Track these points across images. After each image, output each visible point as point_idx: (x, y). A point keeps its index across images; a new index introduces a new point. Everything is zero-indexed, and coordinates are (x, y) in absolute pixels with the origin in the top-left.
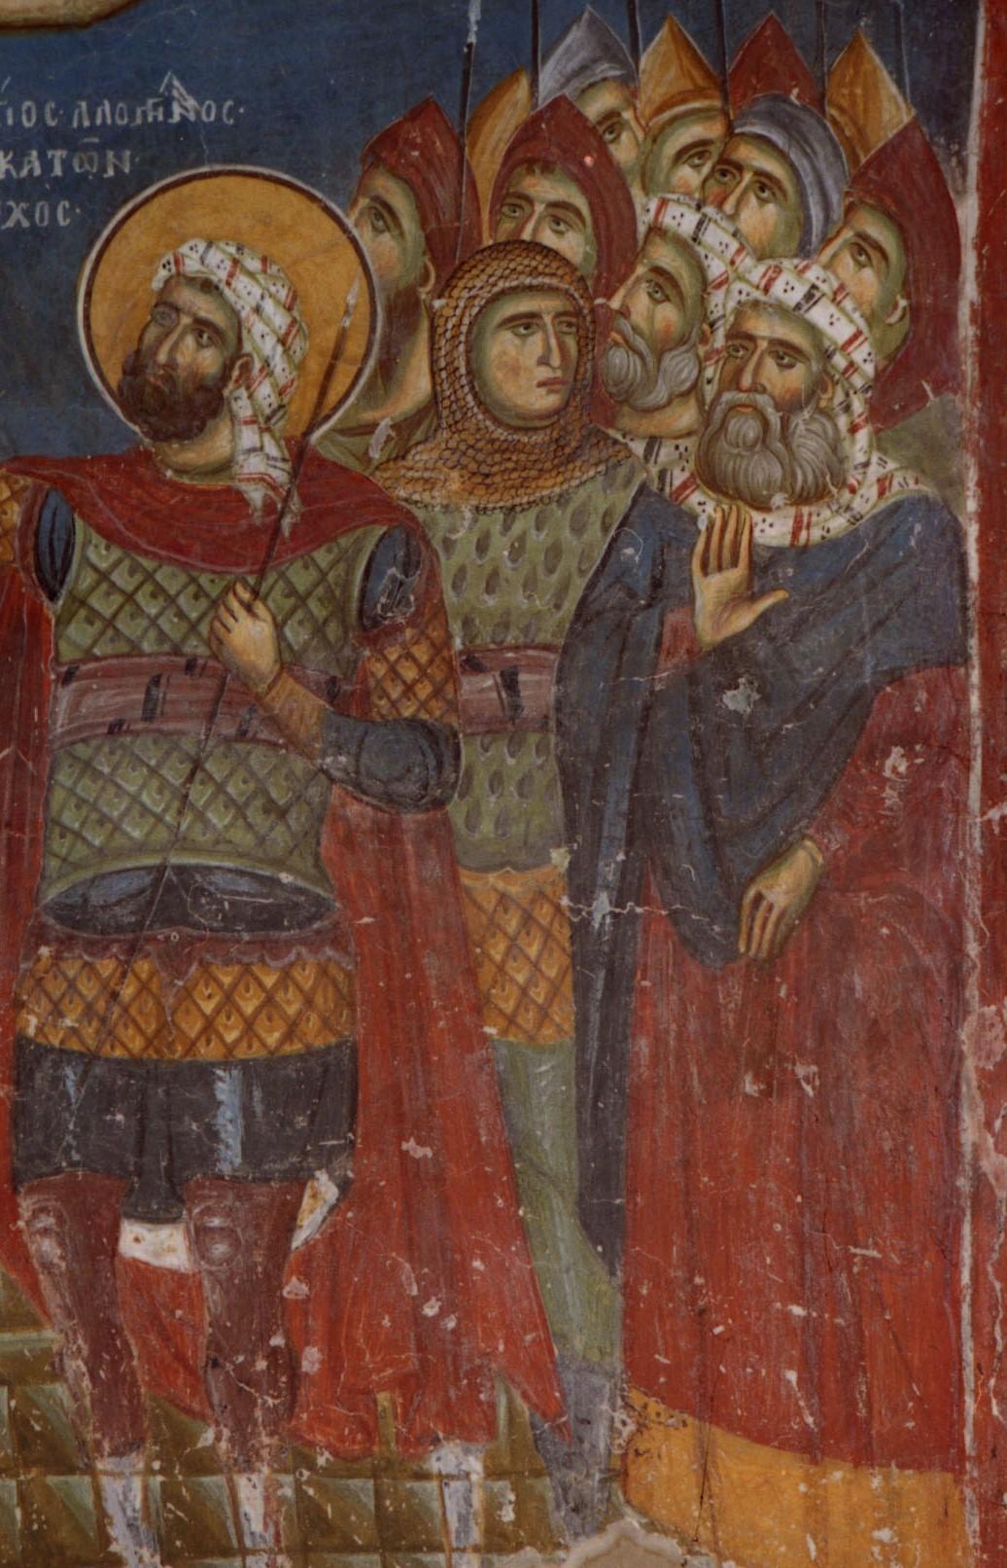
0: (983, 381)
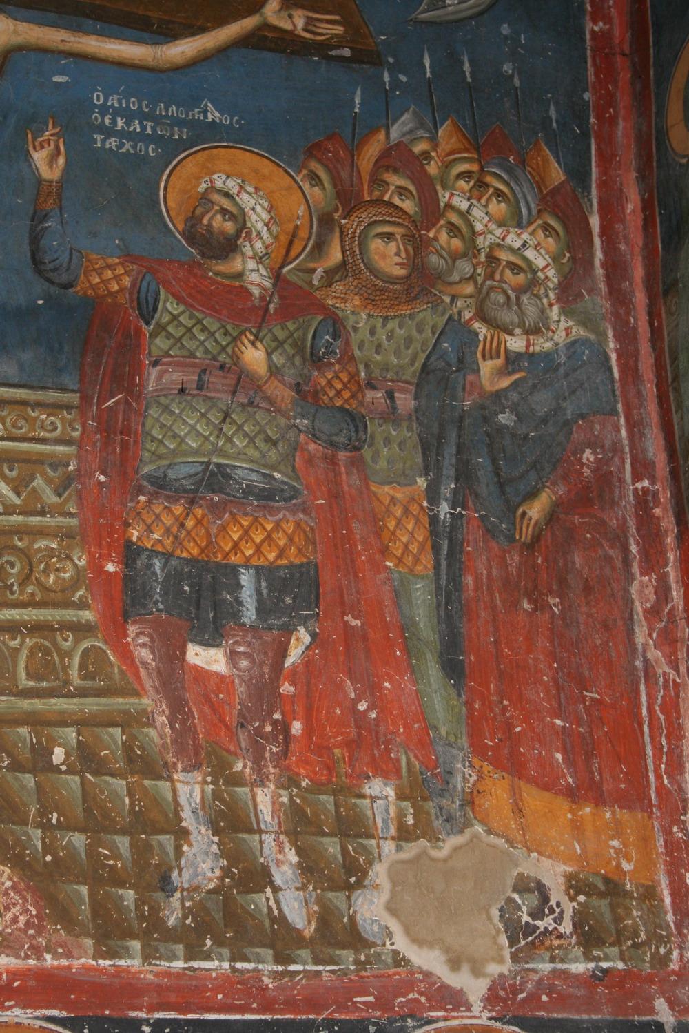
0: (610, 293)
